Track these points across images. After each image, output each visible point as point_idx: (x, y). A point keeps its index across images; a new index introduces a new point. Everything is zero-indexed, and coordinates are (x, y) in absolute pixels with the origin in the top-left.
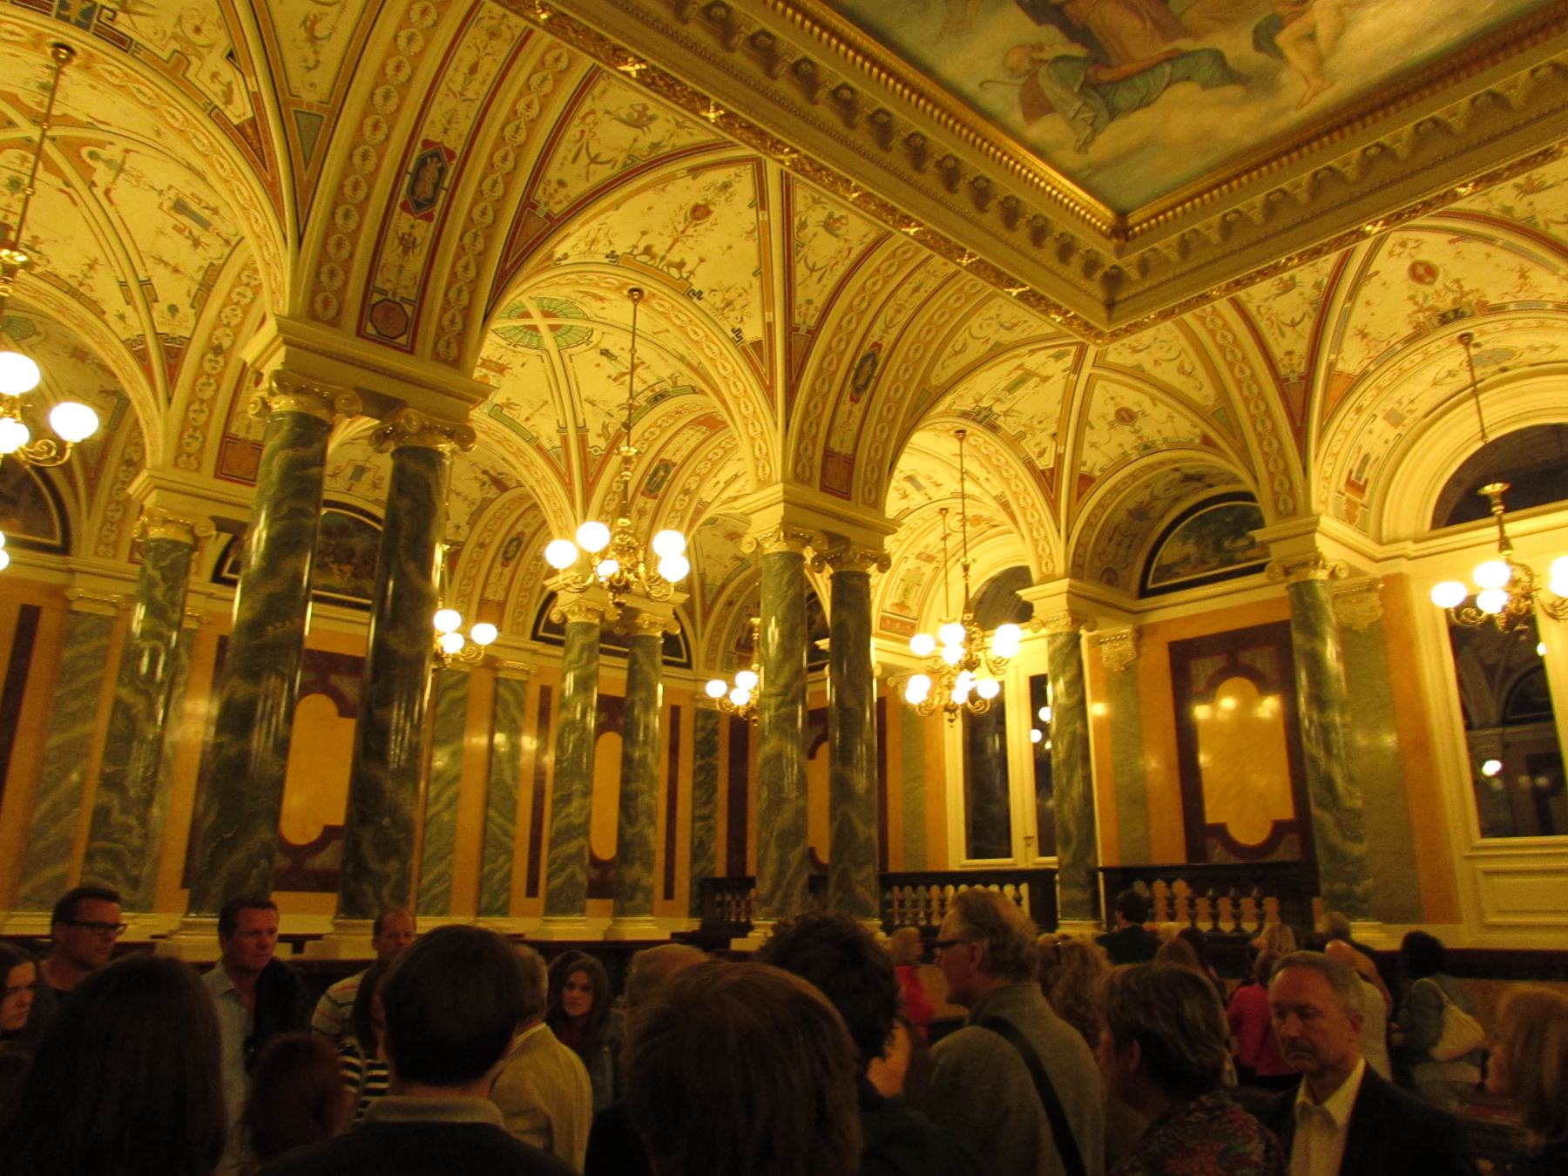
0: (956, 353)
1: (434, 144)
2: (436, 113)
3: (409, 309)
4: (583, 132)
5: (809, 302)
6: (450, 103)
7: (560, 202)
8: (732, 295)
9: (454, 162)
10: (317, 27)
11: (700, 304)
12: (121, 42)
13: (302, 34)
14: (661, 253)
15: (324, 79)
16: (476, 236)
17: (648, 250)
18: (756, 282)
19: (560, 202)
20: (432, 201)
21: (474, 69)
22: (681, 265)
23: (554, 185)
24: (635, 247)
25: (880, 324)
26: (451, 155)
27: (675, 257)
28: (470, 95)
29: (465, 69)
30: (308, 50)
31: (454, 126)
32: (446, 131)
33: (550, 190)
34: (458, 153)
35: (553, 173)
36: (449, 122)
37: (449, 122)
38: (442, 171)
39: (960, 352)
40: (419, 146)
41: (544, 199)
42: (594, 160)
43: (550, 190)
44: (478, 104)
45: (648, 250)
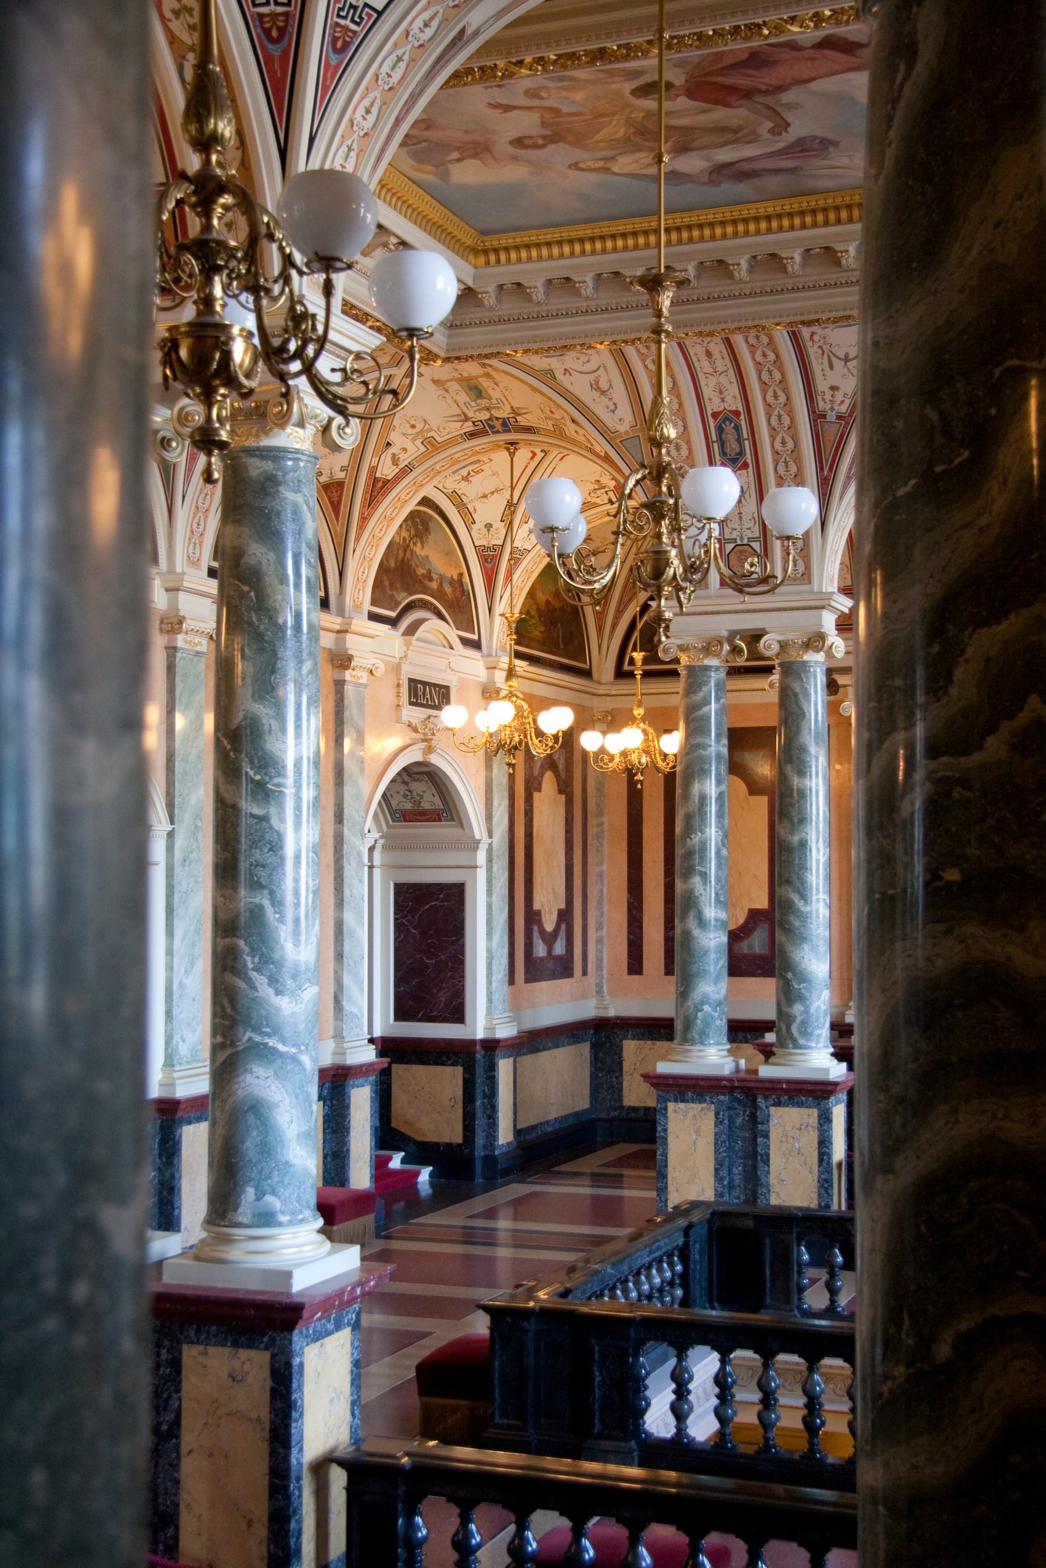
1: (720, 413)
2: (707, 392)
3: (756, 546)
4: (820, 347)
6: (712, 381)
7: (843, 402)
9: (742, 417)
10: (601, 384)
12: (529, 430)
13: (596, 394)
16: (786, 463)
19: (843, 402)
20: (741, 453)
21: (709, 354)
26: (737, 413)
28: (721, 369)
29: (703, 358)
30: (605, 401)
31: (725, 393)
32: (723, 400)
33: (828, 397)
34: (740, 409)
35: (821, 385)
36: (721, 393)
37: (721, 393)
38: (737, 428)
40: (711, 420)
41: (828, 407)
42: (846, 359)
43: (828, 397)
44: (731, 371)
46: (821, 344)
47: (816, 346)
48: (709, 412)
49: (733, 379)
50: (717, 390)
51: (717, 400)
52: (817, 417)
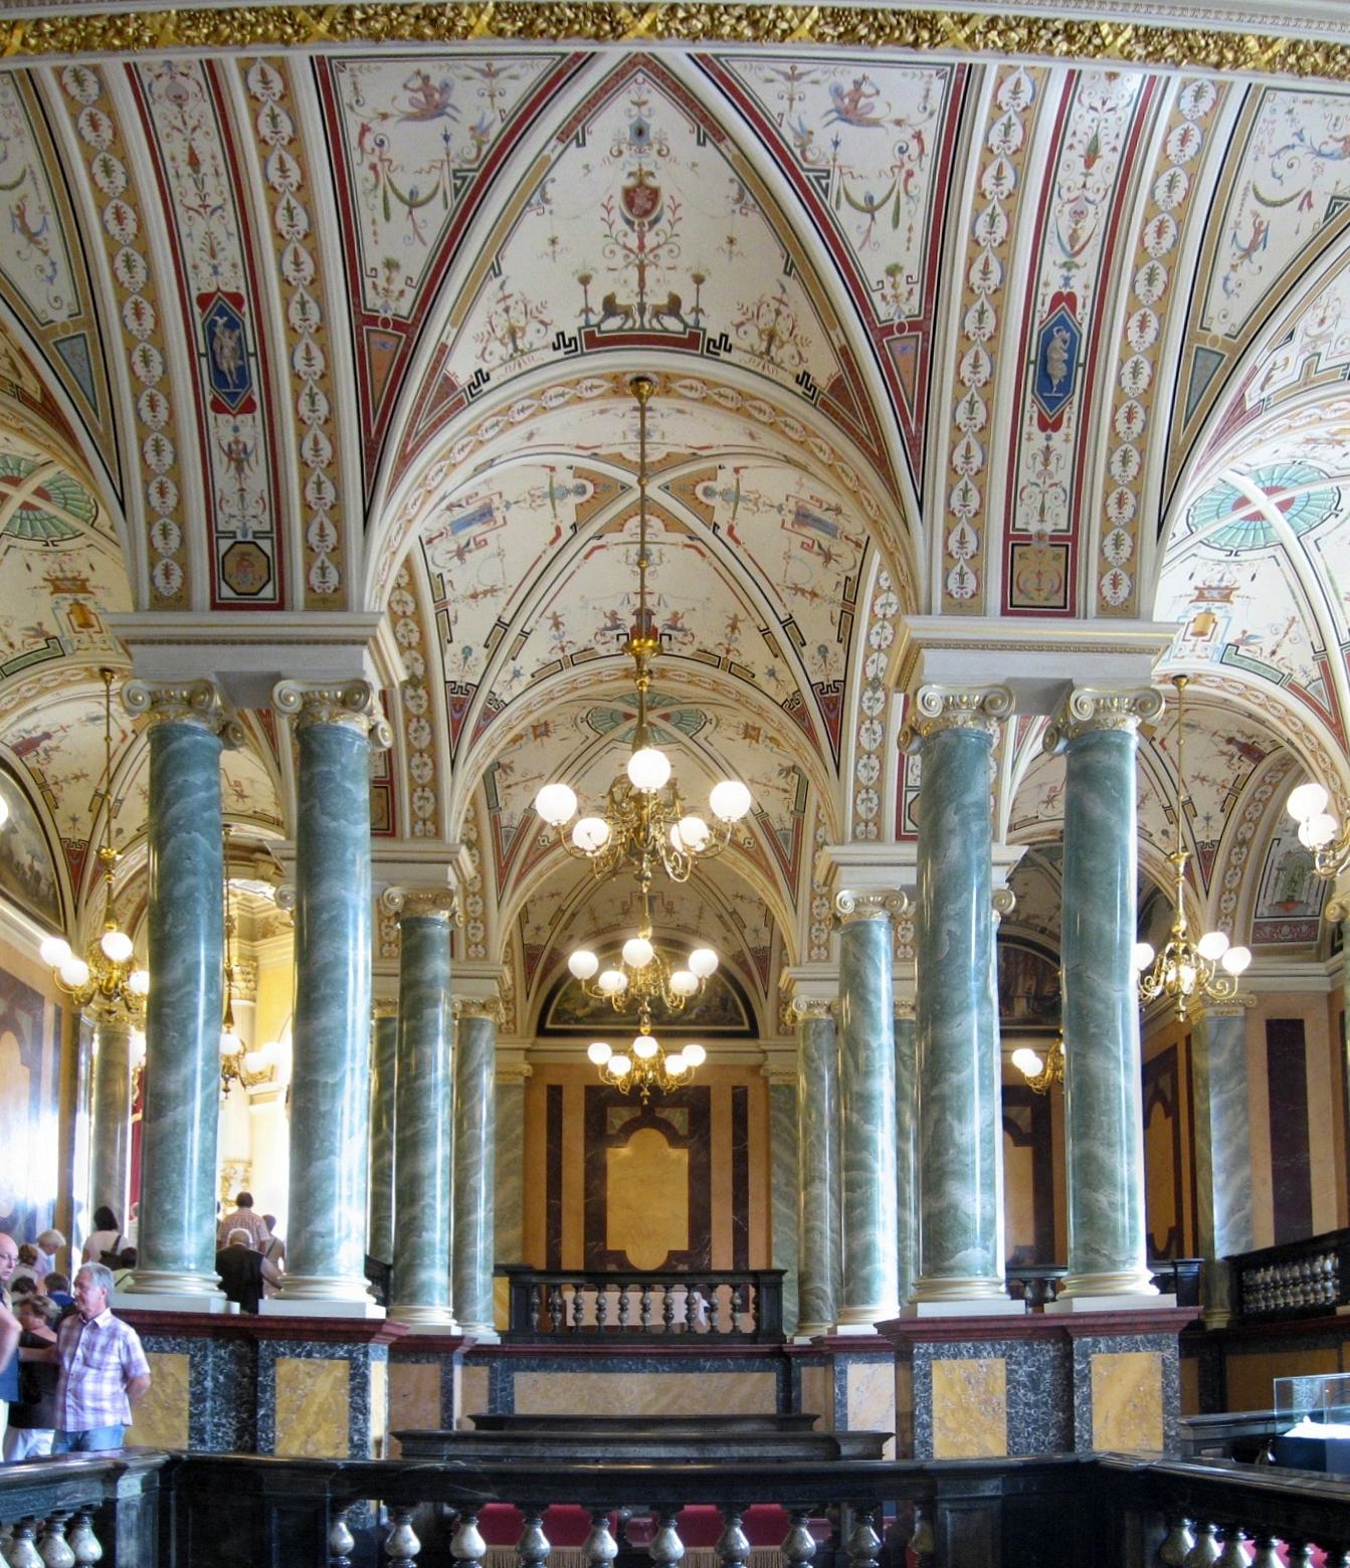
0: (1247, 253)
2: (192, 250)
5: (892, 271)
8: (767, 319)
11: (734, 357)
14: (634, 301)
15: (63, 286)
17: (610, 307)
18: (792, 284)
22: (674, 306)
23: (383, 273)
24: (587, 310)
25: (1053, 255)
26: (237, 299)
27: (658, 298)
31: (220, 256)
32: (215, 271)
33: (381, 282)
36: (213, 255)
37: (213, 255)
39: (1253, 246)
40: (197, 310)
45: (610, 307)
46: (375, 159)
47: (366, 164)
48: (195, 294)
49: (233, 227)
50: (207, 249)
51: (206, 270)
52: (363, 320)
